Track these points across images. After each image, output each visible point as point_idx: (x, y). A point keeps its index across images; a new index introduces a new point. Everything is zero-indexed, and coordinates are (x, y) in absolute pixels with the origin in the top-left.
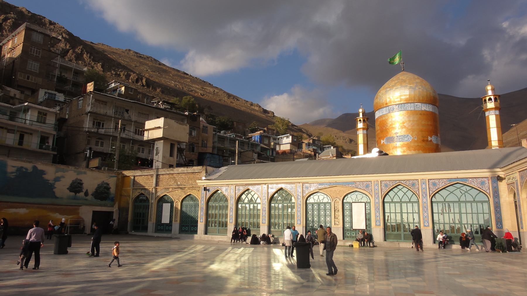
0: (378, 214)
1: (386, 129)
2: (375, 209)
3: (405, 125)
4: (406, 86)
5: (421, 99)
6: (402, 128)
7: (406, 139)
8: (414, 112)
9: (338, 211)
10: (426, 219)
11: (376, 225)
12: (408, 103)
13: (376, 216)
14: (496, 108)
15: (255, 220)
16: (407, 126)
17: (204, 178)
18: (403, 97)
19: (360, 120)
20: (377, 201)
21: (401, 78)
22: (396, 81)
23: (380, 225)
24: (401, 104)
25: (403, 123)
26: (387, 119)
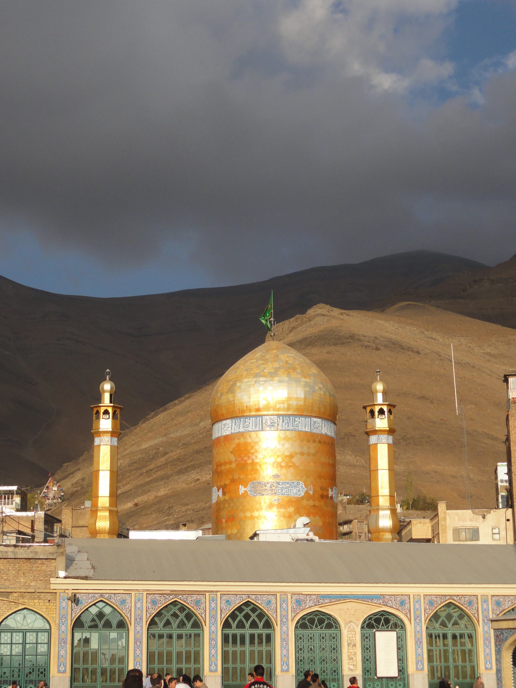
0: (419, 651)
1: (253, 463)
2: (416, 643)
3: (294, 460)
4: (298, 381)
5: (322, 410)
6: (288, 466)
7: (295, 491)
8: (310, 437)
9: (354, 645)
10: (488, 658)
11: (417, 669)
12: (302, 416)
13: (418, 655)
14: (391, 431)
15: (192, 666)
16: (297, 464)
17: (62, 574)
18: (294, 403)
19: (106, 412)
20: (418, 628)
21: (282, 357)
22: (276, 365)
23: (422, 669)
24: (289, 415)
25: (291, 456)
26: (256, 443)
